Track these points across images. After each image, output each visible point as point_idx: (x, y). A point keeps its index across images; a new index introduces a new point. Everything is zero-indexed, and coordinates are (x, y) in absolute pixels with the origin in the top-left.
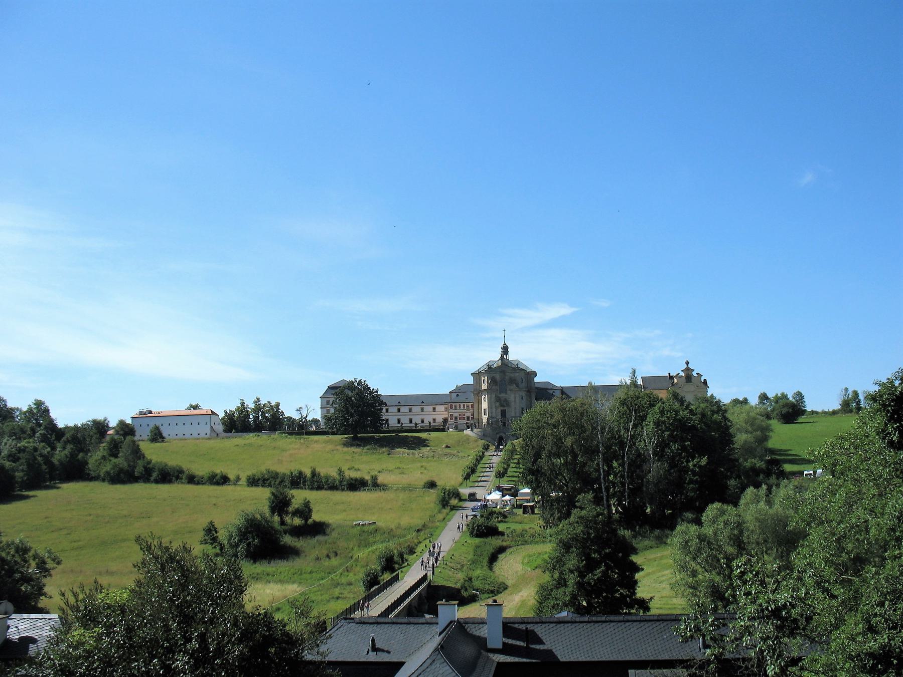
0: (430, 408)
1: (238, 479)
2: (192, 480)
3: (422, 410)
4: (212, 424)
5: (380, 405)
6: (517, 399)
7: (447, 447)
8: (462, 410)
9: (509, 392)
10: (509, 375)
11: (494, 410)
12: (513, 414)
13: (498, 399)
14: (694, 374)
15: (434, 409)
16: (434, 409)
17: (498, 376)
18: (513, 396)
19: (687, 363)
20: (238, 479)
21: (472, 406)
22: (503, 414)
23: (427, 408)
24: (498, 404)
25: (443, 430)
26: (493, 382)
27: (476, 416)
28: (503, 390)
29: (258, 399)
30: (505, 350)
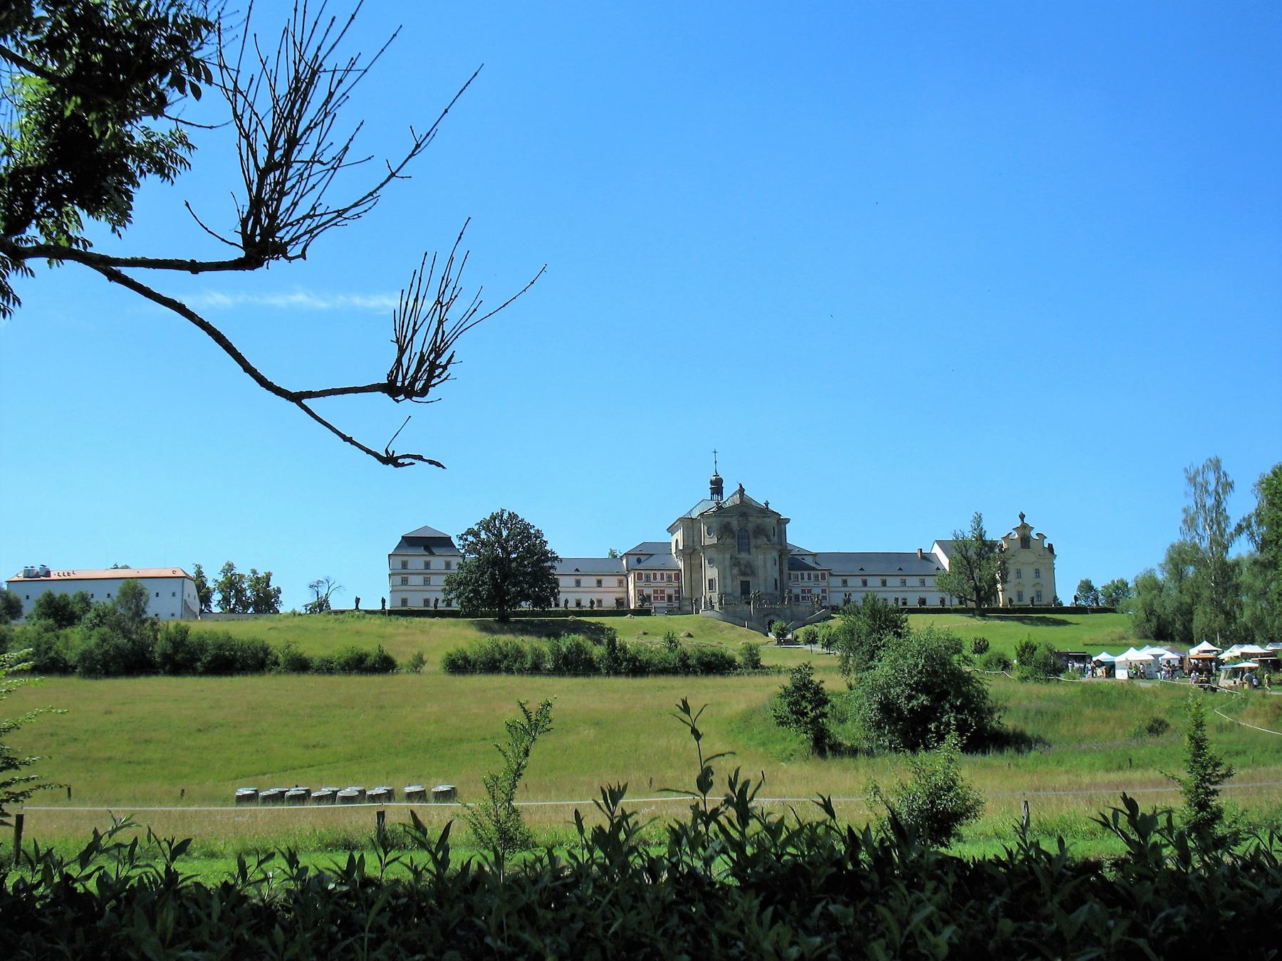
0: (593, 580)
1: (418, 663)
2: (300, 665)
3: (578, 583)
4: (186, 597)
5: (548, 559)
6: (770, 564)
7: (690, 636)
8: (659, 584)
9: (753, 550)
10: (754, 521)
11: (729, 582)
12: (762, 589)
13: (736, 563)
14: (1033, 534)
15: (599, 582)
16: (599, 582)
17: (735, 523)
18: (761, 557)
19: (1022, 517)
20: (418, 663)
21: (678, 577)
22: (745, 588)
23: (585, 581)
24: (736, 571)
25: (647, 613)
26: (725, 531)
27: (685, 593)
28: (744, 545)
29: (230, 567)
30: (717, 487)
